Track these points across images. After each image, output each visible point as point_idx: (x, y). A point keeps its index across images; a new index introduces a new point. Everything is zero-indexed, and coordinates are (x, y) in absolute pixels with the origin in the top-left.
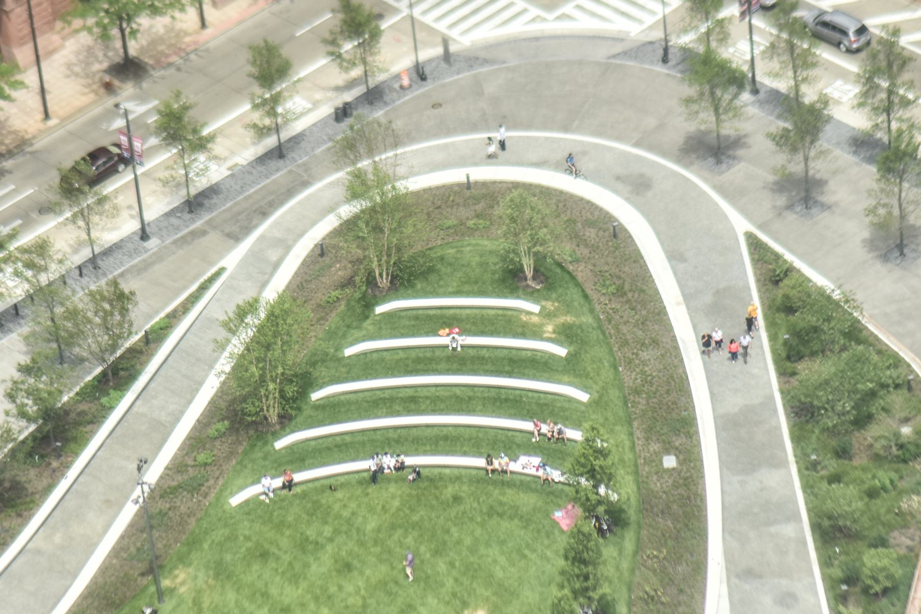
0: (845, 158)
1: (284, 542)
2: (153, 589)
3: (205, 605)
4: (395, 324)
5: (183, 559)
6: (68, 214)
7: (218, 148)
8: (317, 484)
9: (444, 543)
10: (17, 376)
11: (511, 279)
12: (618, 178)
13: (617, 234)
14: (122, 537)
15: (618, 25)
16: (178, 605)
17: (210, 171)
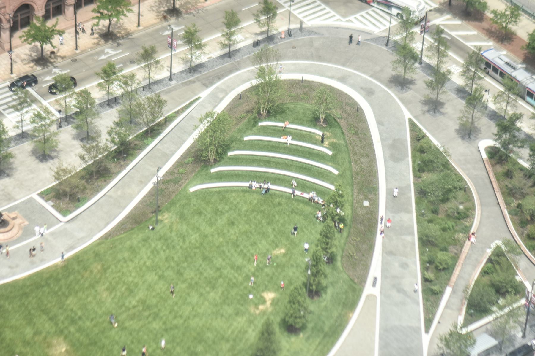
0: (453, 95)
1: (209, 209)
2: (154, 219)
3: (174, 229)
4: (265, 131)
5: (168, 210)
6: (143, 65)
7: (206, 49)
8: (225, 189)
9: (272, 220)
10: (113, 126)
11: (315, 121)
12: (362, 88)
13: (359, 110)
14: (145, 197)
15: (370, 28)
16: (163, 227)
17: (201, 58)
